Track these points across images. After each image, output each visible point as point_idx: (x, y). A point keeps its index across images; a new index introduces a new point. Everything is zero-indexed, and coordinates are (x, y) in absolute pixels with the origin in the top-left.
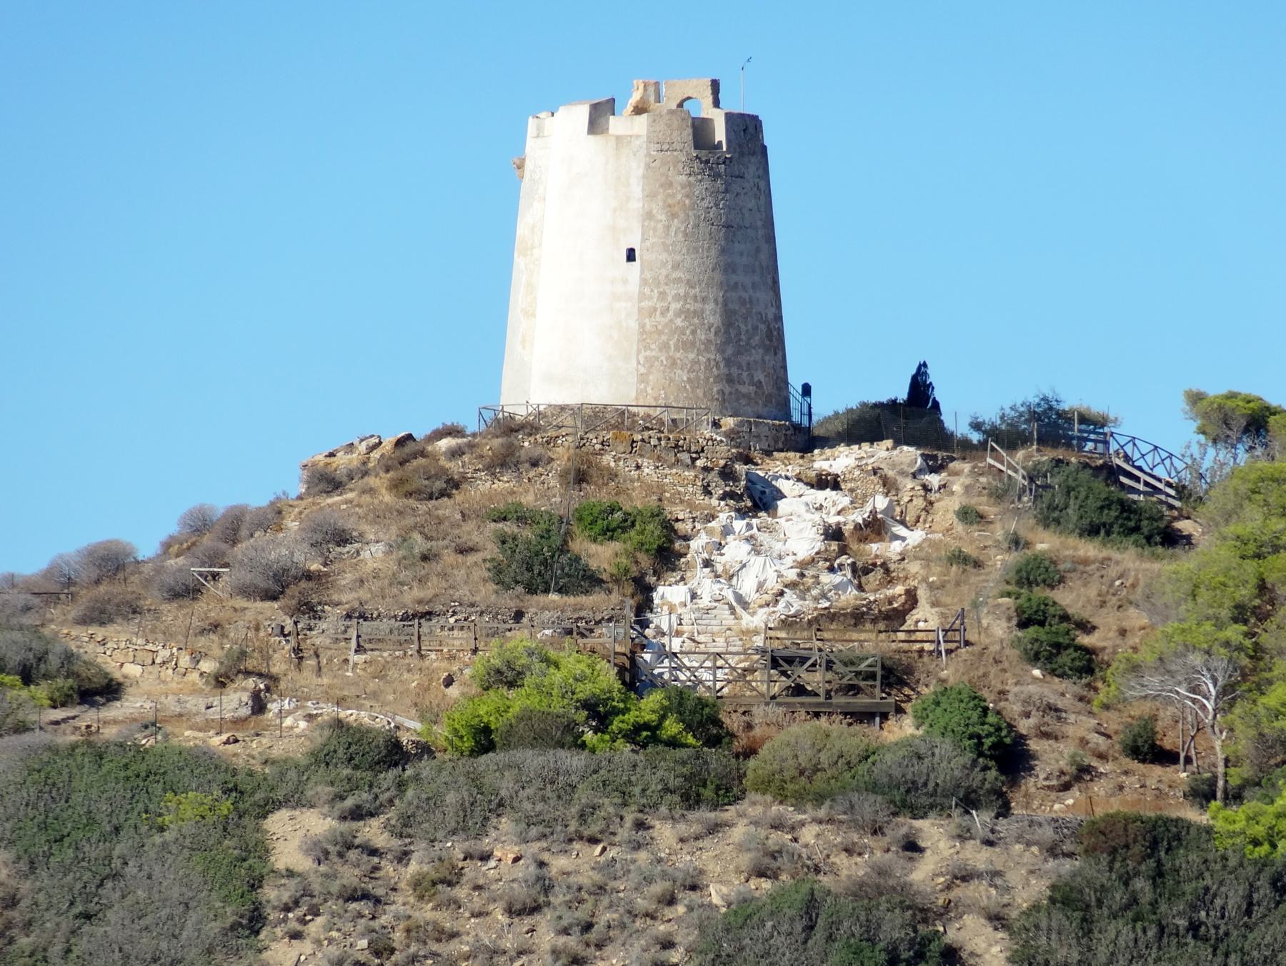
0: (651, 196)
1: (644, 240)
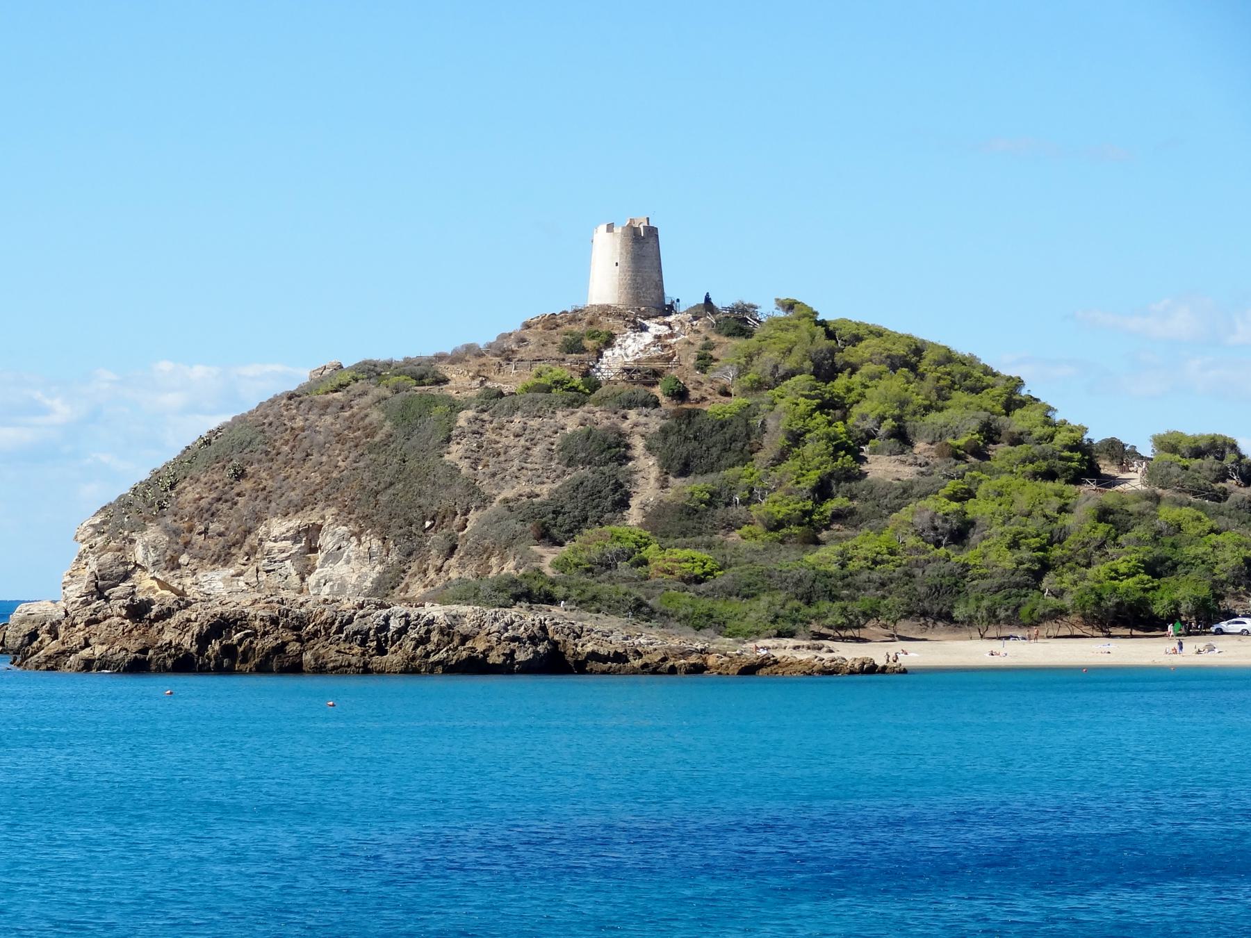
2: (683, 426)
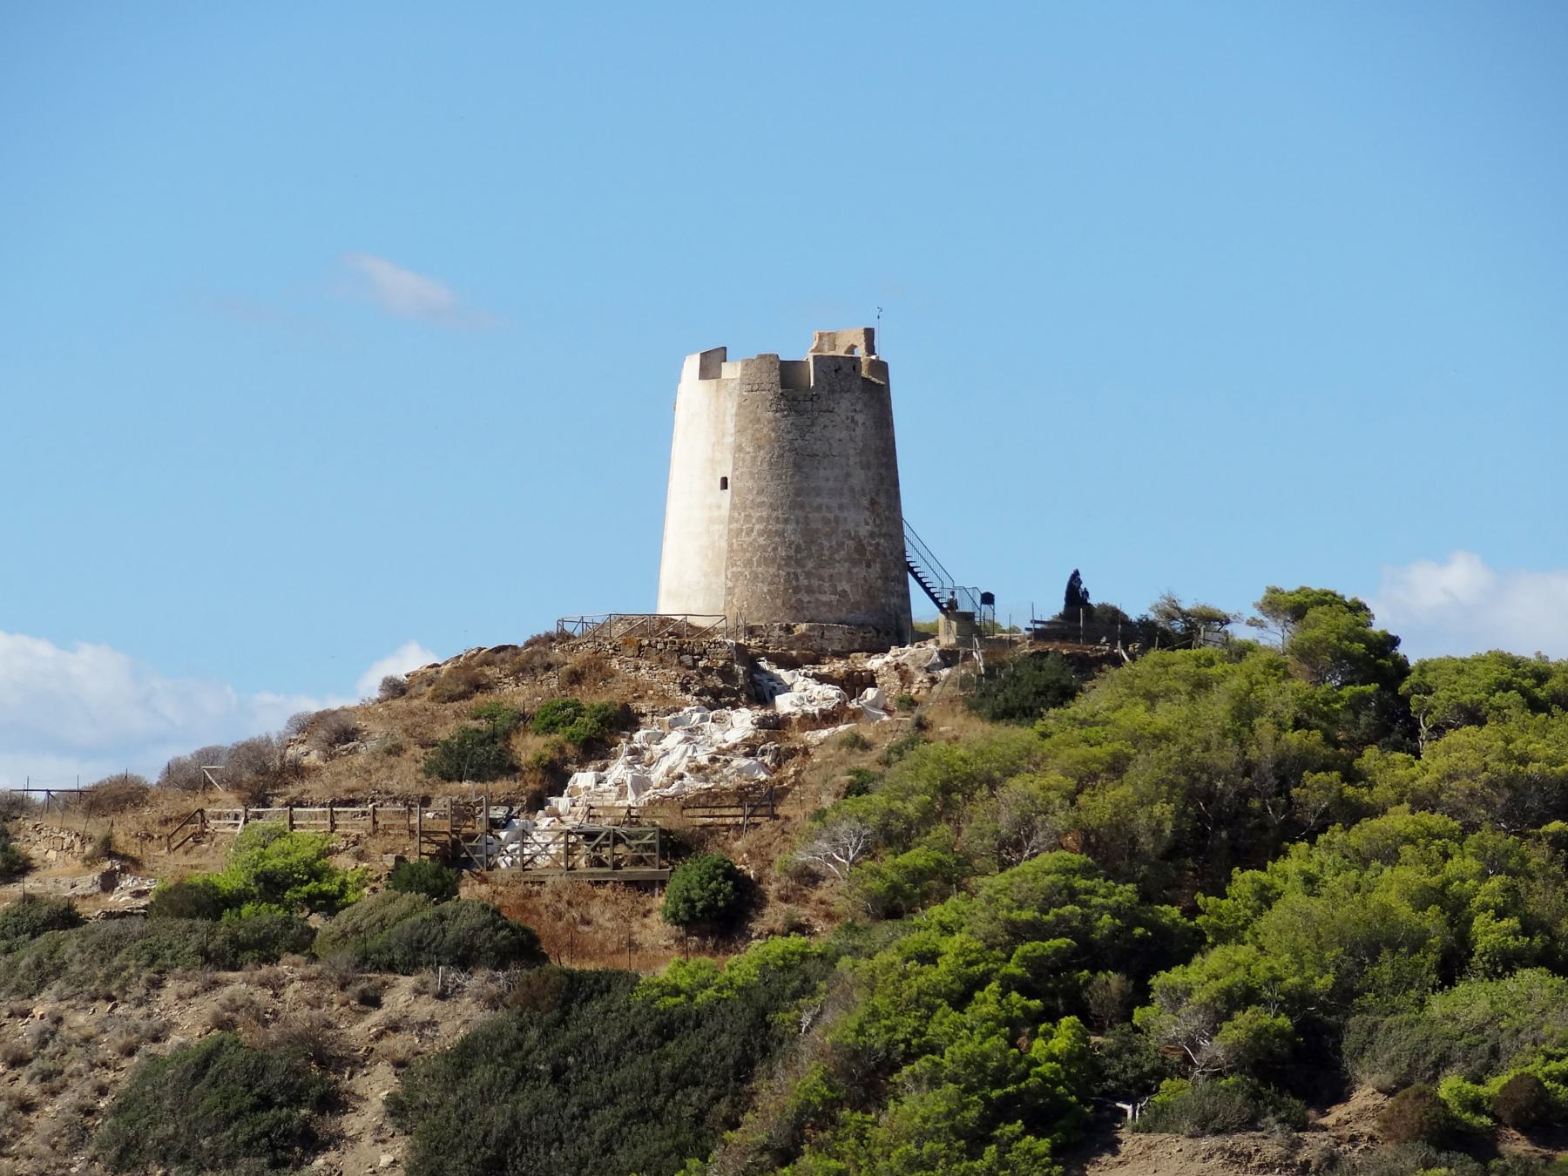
0: (740, 431)
1: (735, 469)
2: (534, 1033)
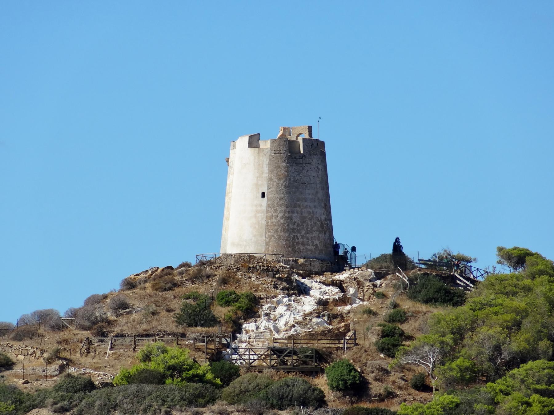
0: (271, 172)
1: (268, 189)
